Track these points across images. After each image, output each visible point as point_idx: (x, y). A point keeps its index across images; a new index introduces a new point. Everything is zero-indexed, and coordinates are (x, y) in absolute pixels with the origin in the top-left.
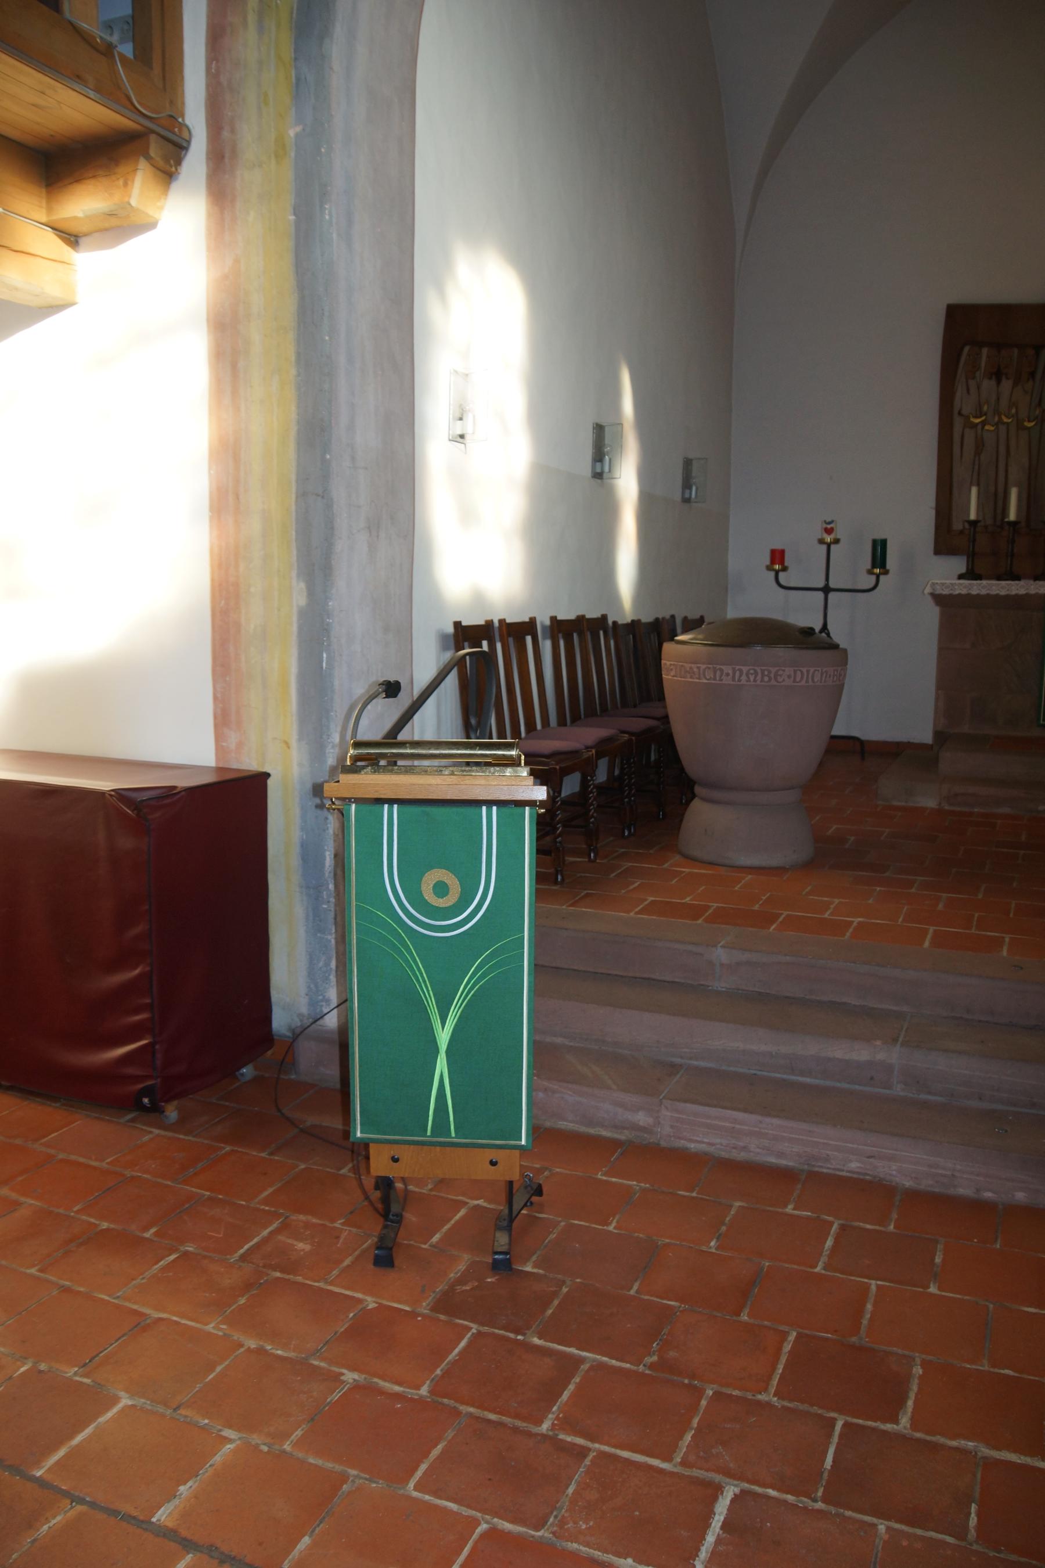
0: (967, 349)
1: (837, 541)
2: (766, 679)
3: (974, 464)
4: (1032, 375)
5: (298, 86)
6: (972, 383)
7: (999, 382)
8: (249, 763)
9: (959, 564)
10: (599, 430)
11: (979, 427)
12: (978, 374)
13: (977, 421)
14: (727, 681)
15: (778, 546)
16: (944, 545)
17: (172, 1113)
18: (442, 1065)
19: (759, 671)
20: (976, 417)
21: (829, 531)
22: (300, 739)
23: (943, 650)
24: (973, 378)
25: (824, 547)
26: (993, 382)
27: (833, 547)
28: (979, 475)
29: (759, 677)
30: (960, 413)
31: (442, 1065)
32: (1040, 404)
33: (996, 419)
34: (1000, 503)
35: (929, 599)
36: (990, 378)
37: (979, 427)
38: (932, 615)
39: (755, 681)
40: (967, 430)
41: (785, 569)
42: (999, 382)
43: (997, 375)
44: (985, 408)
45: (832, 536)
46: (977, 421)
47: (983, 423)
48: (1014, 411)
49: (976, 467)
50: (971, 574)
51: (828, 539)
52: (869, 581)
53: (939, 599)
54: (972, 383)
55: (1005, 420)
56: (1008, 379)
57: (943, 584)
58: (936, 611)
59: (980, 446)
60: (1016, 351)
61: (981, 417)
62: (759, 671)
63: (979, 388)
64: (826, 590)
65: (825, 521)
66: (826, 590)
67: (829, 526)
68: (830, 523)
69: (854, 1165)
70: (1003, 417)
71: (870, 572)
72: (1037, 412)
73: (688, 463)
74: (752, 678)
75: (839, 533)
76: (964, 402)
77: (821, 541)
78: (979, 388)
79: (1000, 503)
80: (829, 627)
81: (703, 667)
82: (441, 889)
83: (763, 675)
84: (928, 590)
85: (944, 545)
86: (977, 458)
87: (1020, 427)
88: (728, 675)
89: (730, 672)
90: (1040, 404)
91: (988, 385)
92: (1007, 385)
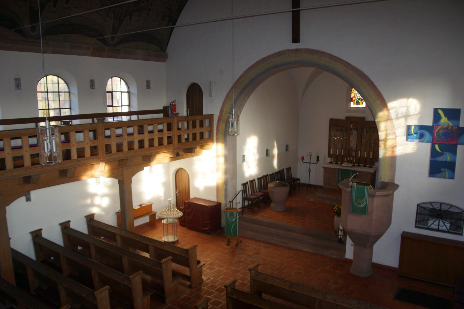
0: (333, 126)
1: (312, 156)
4: (342, 131)
5: (224, 140)
7: (337, 131)
8: (220, 201)
10: (267, 151)
15: (303, 156)
16: (329, 157)
17: (212, 234)
18: (232, 230)
20: (334, 137)
21: (310, 154)
23: (324, 175)
25: (309, 157)
27: (311, 157)
31: (232, 230)
32: (343, 136)
35: (322, 168)
38: (322, 170)
41: (304, 159)
42: (337, 131)
43: (337, 130)
47: (335, 138)
50: (331, 163)
51: (310, 155)
52: (316, 162)
53: (323, 168)
54: (333, 132)
58: (323, 169)
64: (310, 163)
66: (310, 163)
71: (316, 161)
73: (287, 146)
77: (309, 156)
82: (232, 218)
84: (321, 166)
85: (329, 157)
90: (343, 136)
91: (336, 132)
92: (338, 132)
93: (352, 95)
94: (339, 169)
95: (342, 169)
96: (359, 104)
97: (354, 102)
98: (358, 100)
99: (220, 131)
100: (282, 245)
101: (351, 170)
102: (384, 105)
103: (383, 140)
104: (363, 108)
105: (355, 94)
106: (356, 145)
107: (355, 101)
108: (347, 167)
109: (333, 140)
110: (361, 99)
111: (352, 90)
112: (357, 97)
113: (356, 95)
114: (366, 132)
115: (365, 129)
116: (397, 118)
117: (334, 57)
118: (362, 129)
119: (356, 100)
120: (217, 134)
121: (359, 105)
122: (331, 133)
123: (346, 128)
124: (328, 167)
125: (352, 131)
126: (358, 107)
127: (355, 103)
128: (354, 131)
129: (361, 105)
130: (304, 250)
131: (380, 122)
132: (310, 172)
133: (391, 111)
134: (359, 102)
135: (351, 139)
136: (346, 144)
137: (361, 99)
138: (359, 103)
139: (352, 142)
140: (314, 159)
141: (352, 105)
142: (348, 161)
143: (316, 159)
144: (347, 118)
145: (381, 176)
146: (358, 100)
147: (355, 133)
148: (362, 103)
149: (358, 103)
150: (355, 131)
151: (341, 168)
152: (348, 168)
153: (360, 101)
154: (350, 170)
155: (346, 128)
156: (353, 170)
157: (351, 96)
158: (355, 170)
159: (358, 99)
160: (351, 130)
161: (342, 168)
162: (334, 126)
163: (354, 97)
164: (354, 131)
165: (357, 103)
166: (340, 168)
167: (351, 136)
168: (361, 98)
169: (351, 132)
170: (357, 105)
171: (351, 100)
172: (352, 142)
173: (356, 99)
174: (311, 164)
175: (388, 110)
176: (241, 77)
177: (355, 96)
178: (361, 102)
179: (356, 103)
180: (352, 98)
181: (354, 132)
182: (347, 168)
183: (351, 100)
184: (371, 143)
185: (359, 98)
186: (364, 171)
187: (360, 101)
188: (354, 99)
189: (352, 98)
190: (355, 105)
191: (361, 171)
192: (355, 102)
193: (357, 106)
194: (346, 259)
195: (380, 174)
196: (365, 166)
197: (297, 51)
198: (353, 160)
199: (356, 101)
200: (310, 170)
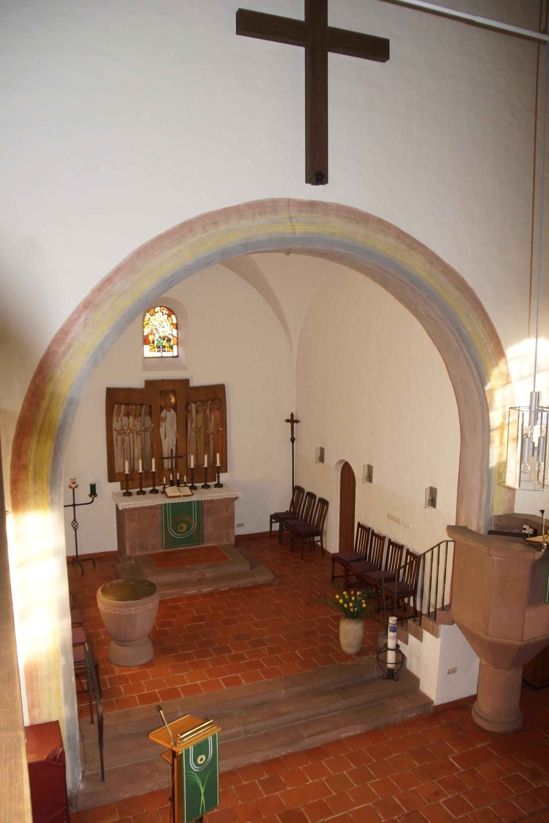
0: (116, 406)
1: (77, 486)
2: (145, 609)
3: (121, 448)
4: (140, 415)
6: (119, 418)
7: (128, 417)
9: (117, 486)
11: (123, 434)
12: (121, 415)
13: (121, 432)
14: (133, 612)
16: (112, 479)
19: (143, 608)
20: (121, 431)
21: (74, 483)
22: (66, 704)
24: (119, 416)
25: (72, 490)
26: (126, 418)
27: (75, 489)
28: (124, 452)
29: (143, 609)
30: (115, 430)
32: (144, 425)
33: (129, 431)
34: (132, 462)
36: (125, 416)
37: (123, 434)
39: (142, 610)
40: (118, 436)
42: (128, 417)
43: (128, 415)
44: (124, 427)
45: (75, 485)
46: (121, 432)
48: (135, 428)
49: (123, 449)
52: (90, 499)
54: (119, 418)
55: (132, 432)
56: (132, 416)
57: (126, 505)
59: (123, 441)
60: (134, 406)
61: (123, 430)
62: (143, 608)
63: (121, 420)
65: (72, 480)
67: (73, 481)
68: (74, 480)
69: (247, 762)
70: (131, 430)
71: (90, 495)
72: (143, 428)
74: (141, 610)
75: (77, 483)
76: (116, 425)
77: (70, 487)
78: (121, 420)
79: (132, 462)
80: (77, 519)
81: (124, 609)
83: (144, 608)
85: (112, 479)
86: (123, 446)
87: (138, 434)
88: (133, 611)
89: (134, 610)
90: (144, 425)
91: (125, 419)
92: (131, 418)
93: (144, 329)
94: (165, 504)
95: (171, 503)
96: (164, 349)
97: (152, 344)
98: (162, 341)
99: (31, 468)
100: (283, 753)
101: (194, 501)
102: (500, 353)
103: (497, 429)
104: (173, 357)
105: (154, 327)
106: (175, 444)
107: (153, 342)
108: (184, 496)
109: (119, 437)
110: (166, 339)
111: (146, 319)
112: (159, 333)
113: (157, 329)
114: (197, 411)
115: (193, 405)
116: (521, 378)
117: (407, 236)
118: (187, 405)
119: (157, 340)
120: (15, 482)
121: (165, 351)
122: (115, 421)
123: (150, 406)
124: (137, 506)
125: (164, 412)
126: (162, 357)
127: (155, 347)
128: (170, 411)
129: (168, 351)
130: (343, 736)
131: (492, 390)
132: (77, 529)
133: (510, 365)
134: (164, 344)
135: (162, 430)
136: (152, 444)
137: (166, 339)
138: (164, 347)
139: (165, 438)
140: (83, 494)
141: (148, 351)
142: (171, 482)
143: (89, 493)
144: (148, 383)
145: (492, 506)
146: (160, 339)
147: (170, 416)
148: (171, 347)
149: (162, 348)
150: (172, 410)
151: (170, 501)
152: (185, 500)
153: (165, 343)
154: (190, 503)
155: (150, 406)
156: (198, 501)
157: (143, 332)
158: (203, 499)
159: (160, 337)
160: (162, 409)
161: (173, 502)
162: (121, 404)
163: (152, 333)
164: (170, 411)
165: (158, 347)
166: (167, 502)
167: (163, 424)
168: (167, 336)
169: (162, 415)
170: (158, 351)
171: (146, 341)
172: (165, 438)
173: (157, 336)
174: (72, 507)
175: (506, 363)
176: (118, 270)
177: (154, 331)
178: (167, 345)
179: (156, 348)
180: (147, 336)
181: (169, 414)
182: (185, 498)
183: (146, 341)
184: (209, 433)
185: (162, 336)
186: (222, 498)
187: (165, 343)
188: (151, 338)
189: (147, 336)
190: (155, 351)
191: (215, 499)
192: (155, 346)
193: (159, 354)
194: (437, 707)
195: (491, 502)
196: (206, 487)
197: (312, 205)
198: (182, 476)
199: (156, 343)
200: (76, 522)
